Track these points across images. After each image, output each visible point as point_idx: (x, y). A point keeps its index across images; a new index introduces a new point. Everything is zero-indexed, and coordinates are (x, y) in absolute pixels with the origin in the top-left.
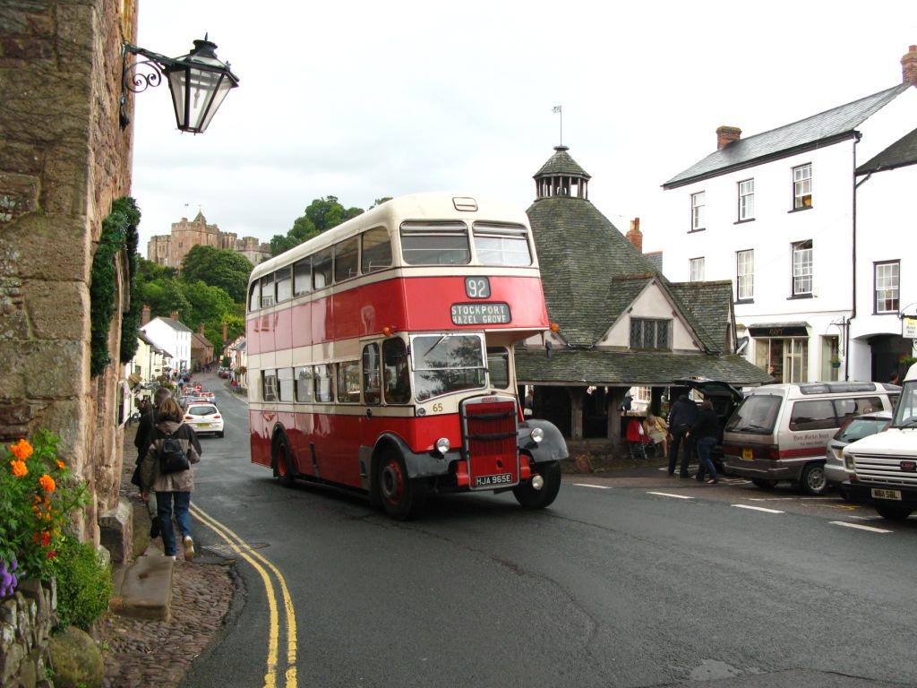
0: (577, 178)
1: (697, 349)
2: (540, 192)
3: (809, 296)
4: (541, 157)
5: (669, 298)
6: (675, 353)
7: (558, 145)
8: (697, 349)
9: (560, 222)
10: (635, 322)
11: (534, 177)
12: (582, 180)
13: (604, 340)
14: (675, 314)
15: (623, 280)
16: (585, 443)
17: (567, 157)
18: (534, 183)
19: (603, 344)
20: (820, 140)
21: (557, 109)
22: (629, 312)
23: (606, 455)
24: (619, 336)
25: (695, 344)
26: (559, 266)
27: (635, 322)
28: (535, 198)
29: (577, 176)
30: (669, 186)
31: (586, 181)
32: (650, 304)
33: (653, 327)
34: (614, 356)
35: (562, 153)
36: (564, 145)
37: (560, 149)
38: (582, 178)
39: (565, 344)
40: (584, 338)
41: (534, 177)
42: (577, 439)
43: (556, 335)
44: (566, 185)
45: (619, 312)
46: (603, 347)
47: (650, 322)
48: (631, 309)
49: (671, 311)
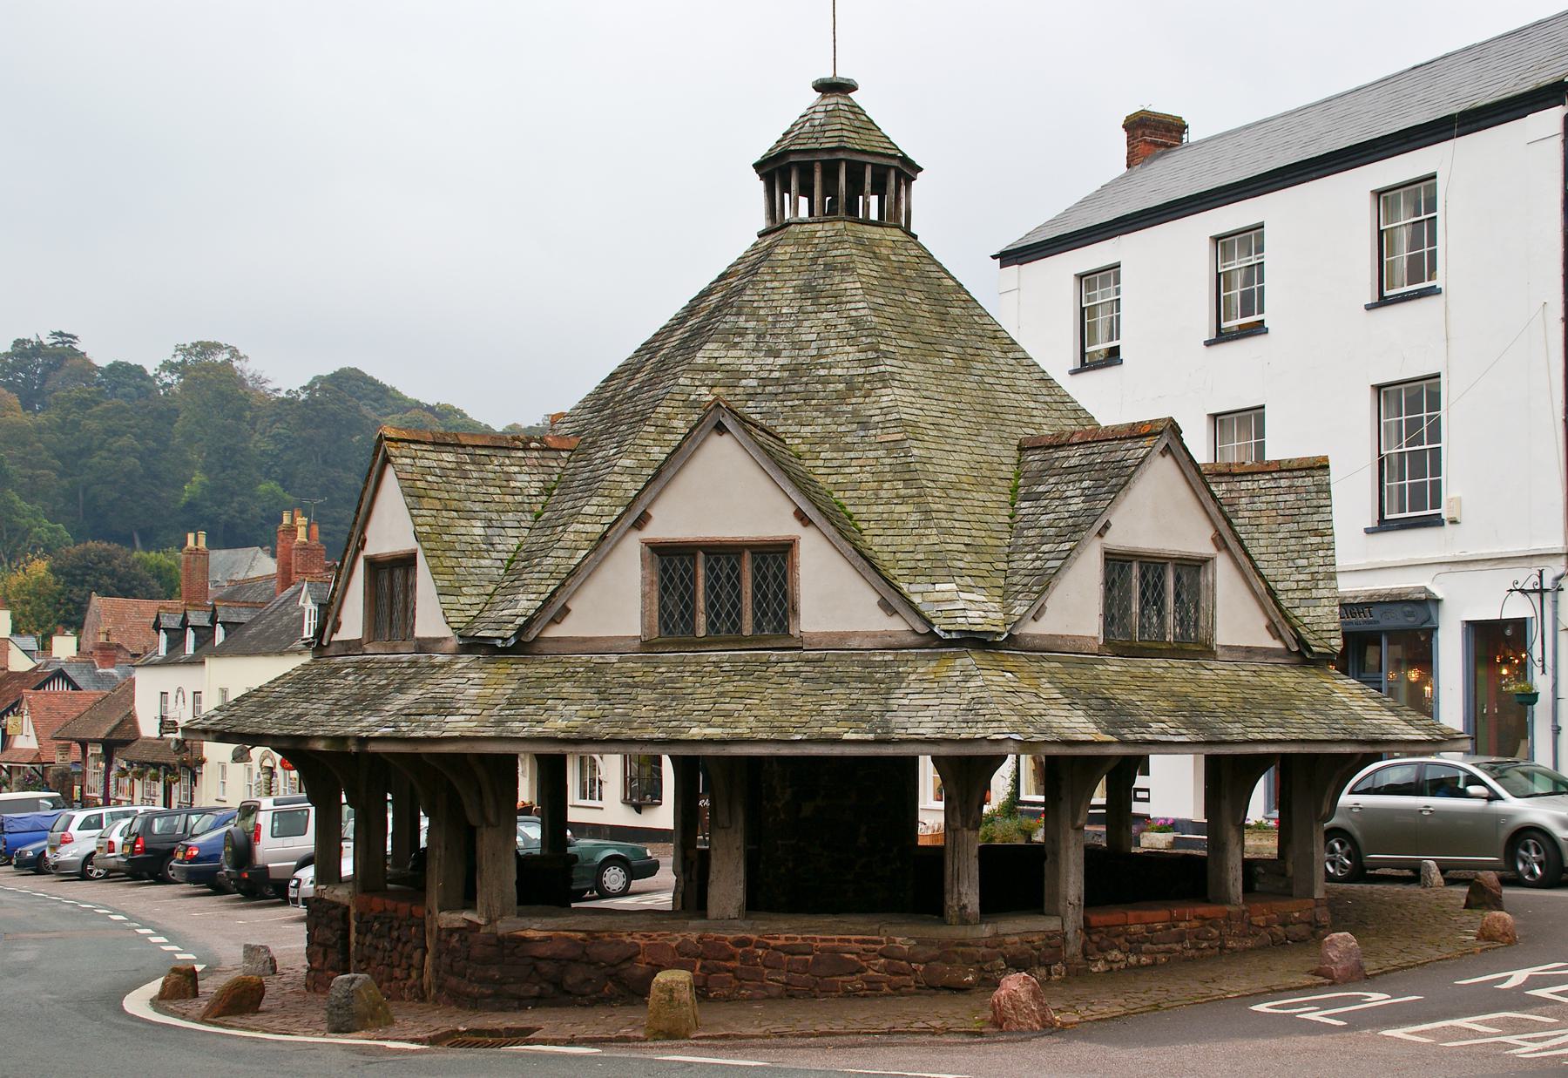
0: (889, 168)
1: (1278, 645)
3: (1435, 522)
4: (780, 110)
5: (1205, 496)
7: (827, 74)
8: (1278, 645)
9: (851, 284)
10: (1116, 563)
12: (899, 174)
14: (1219, 542)
16: (986, 930)
17: (856, 110)
19: (1031, 629)
20: (1463, 114)
22: (1100, 535)
23: (1048, 966)
25: (1273, 629)
27: (1116, 563)
28: (762, 223)
29: (885, 161)
30: (1008, 257)
31: (910, 180)
32: (1156, 517)
33: (1161, 576)
36: (844, 74)
37: (833, 88)
38: (898, 172)
40: (975, 609)
43: (895, 601)
44: (856, 188)
45: (1074, 531)
46: (1034, 637)
47: (1153, 565)
48: (1107, 526)
49: (1210, 532)
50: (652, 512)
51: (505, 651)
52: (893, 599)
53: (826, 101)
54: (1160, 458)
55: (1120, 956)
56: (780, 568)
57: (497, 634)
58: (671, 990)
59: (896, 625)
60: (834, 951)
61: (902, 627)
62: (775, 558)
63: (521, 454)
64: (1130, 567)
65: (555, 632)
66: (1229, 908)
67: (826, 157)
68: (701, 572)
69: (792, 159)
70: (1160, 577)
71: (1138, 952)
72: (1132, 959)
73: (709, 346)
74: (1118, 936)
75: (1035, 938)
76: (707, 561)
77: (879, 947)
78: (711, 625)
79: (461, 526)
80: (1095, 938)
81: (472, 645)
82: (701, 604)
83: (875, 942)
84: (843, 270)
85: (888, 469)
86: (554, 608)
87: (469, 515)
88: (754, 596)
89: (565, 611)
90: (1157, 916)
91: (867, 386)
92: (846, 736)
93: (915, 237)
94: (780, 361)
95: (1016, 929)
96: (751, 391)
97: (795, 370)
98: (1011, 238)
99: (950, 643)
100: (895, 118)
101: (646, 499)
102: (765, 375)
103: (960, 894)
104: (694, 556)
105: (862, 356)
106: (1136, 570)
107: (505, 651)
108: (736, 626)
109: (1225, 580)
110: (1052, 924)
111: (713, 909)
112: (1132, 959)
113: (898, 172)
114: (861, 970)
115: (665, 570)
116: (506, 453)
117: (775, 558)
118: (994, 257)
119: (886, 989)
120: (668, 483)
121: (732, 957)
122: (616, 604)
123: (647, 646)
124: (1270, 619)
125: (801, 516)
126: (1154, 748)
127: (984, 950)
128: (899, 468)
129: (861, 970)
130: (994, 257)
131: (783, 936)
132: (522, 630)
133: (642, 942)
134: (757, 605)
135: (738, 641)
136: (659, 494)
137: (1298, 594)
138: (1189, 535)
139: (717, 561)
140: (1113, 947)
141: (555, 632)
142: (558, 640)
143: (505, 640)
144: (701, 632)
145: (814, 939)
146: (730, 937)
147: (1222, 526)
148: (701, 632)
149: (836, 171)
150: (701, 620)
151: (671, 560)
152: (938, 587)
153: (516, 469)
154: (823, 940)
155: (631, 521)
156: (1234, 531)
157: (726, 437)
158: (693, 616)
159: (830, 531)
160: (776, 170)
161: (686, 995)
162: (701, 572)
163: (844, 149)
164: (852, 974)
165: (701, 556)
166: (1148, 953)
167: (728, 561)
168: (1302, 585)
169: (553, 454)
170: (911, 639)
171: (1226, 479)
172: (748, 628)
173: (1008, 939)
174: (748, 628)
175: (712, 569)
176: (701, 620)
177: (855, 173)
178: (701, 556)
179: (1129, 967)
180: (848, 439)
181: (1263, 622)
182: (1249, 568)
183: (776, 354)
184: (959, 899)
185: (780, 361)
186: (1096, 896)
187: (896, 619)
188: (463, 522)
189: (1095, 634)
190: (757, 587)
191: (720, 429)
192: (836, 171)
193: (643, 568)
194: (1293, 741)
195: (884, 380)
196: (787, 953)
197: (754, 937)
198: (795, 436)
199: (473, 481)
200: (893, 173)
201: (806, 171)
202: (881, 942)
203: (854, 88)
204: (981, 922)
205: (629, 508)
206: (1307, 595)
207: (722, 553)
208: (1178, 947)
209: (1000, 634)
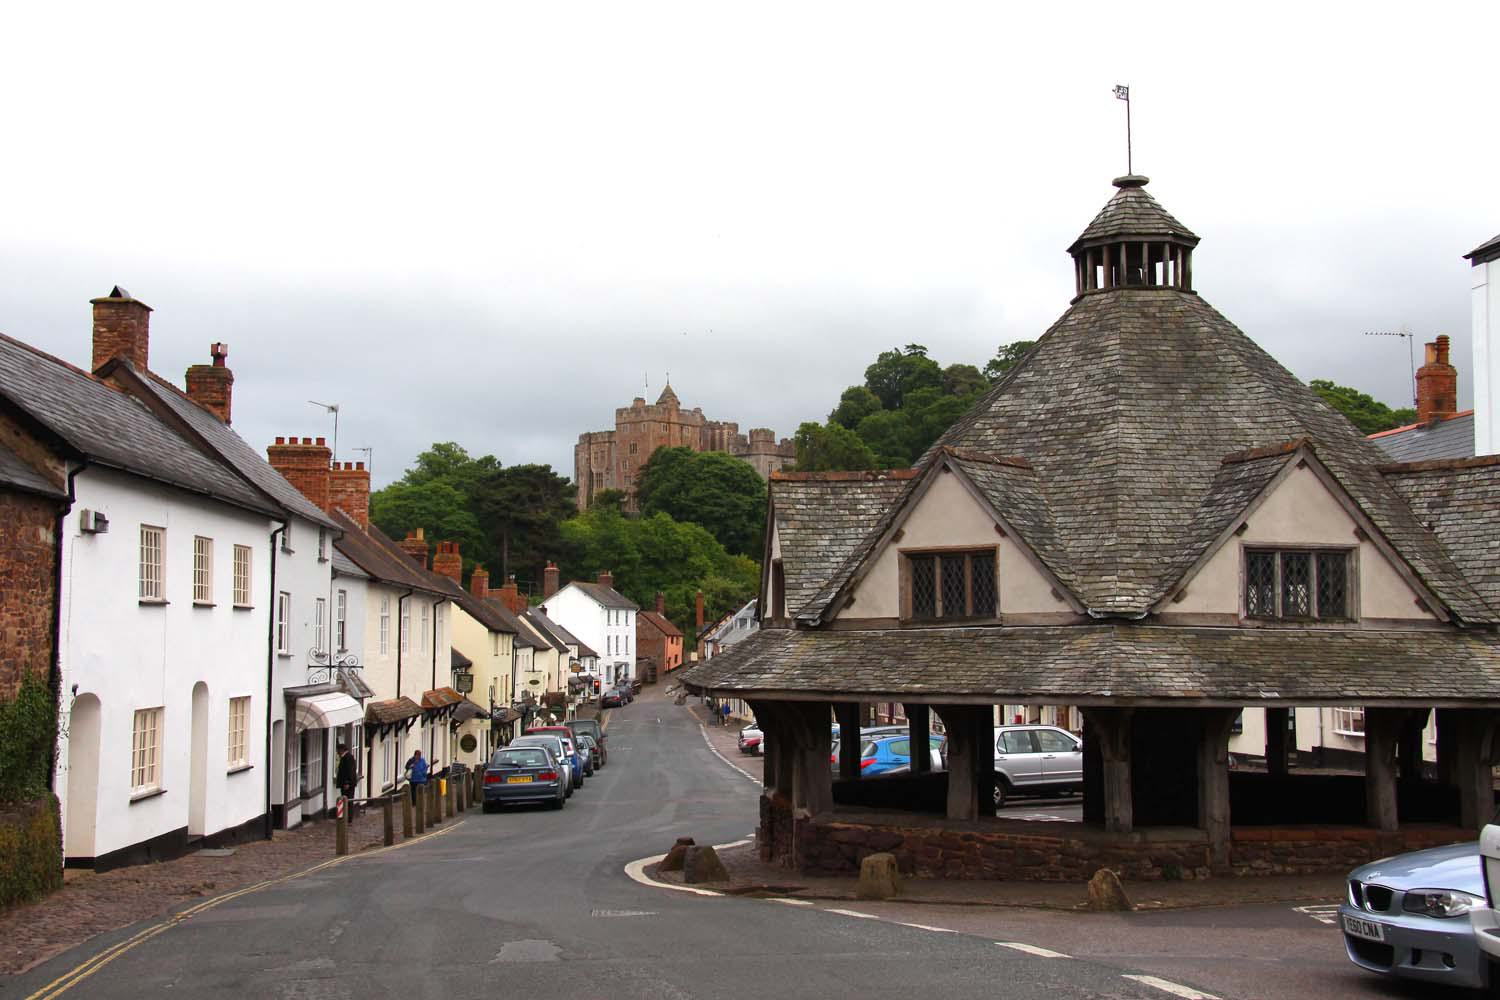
1: (1428, 616)
2: (1085, 279)
4: (1087, 203)
6: (1365, 626)
7: (1123, 173)
8: (1428, 616)
9: (1112, 342)
11: (1069, 250)
13: (1177, 600)
14: (1361, 534)
15: (1242, 462)
16: (1137, 838)
17: (1144, 199)
18: (1071, 262)
19: (1173, 608)
21: (1122, 92)
24: (1217, 589)
25: (1421, 603)
26: (1097, 440)
31: (1187, 252)
34: (1207, 637)
35: (1131, 193)
37: (1130, 184)
38: (1183, 244)
39: (1081, 611)
41: (1069, 250)
42: (1118, 830)
43: (1062, 591)
45: (1215, 535)
48: (1244, 527)
49: (1353, 527)
50: (906, 529)
51: (815, 628)
52: (1062, 590)
53: (1124, 195)
54: (1297, 470)
55: (1264, 865)
56: (990, 567)
57: (811, 617)
58: (873, 867)
59: (1064, 608)
60: (1027, 848)
61: (1067, 609)
62: (985, 558)
63: (871, 485)
64: (1273, 559)
65: (845, 615)
66: (1379, 832)
67: (1110, 241)
68: (938, 571)
69: (1086, 245)
70: (1303, 564)
71: (1284, 864)
72: (1278, 868)
73: (1005, 397)
74: (1264, 849)
75: (1180, 845)
76: (942, 563)
77: (1058, 846)
78: (945, 608)
79: (814, 540)
80: (1240, 849)
81: (803, 626)
82: (938, 595)
83: (1056, 842)
84: (1112, 330)
85: (1096, 487)
86: (847, 596)
87: (819, 533)
88: (973, 588)
89: (851, 601)
90: (1305, 836)
91: (1102, 422)
92: (998, 691)
93: (1195, 293)
94: (1048, 406)
95: (1165, 840)
96: (1022, 430)
97: (1056, 413)
98: (1475, 246)
99: (1101, 621)
100: (1177, 198)
101: (899, 519)
102: (1033, 417)
103: (1114, 809)
104: (933, 559)
105: (1104, 399)
106: (1278, 560)
107: (815, 628)
108: (962, 609)
109: (1370, 568)
110: (1195, 835)
111: (951, 813)
112: (1278, 868)
113: (1183, 244)
114: (1045, 863)
115: (916, 570)
116: (858, 485)
117: (985, 558)
118: (1466, 257)
119: (1062, 878)
120: (913, 509)
121: (960, 848)
122: (884, 594)
123: (903, 623)
124: (1418, 595)
125: (999, 529)
126: (1244, 703)
127: (1132, 853)
128: (1104, 487)
129: (1045, 863)
130: (1466, 257)
131: (997, 835)
132: (823, 615)
133: (906, 835)
134: (975, 594)
135: (963, 620)
136: (909, 515)
137: (1483, 572)
138: (1330, 528)
139: (949, 563)
140: (1258, 857)
141: (845, 615)
142: (848, 620)
143: (814, 620)
144: (939, 614)
145: (1016, 838)
146: (961, 834)
147: (1363, 522)
148: (939, 614)
149: (1131, 248)
150: (939, 605)
151: (918, 562)
152: (1104, 578)
153: (864, 496)
154: (1022, 839)
155: (890, 536)
156: (1374, 525)
157: (950, 475)
158: (934, 603)
159: (1017, 539)
160: (1085, 252)
161: (884, 869)
162: (938, 571)
163: (1121, 234)
164: (1039, 865)
165: (938, 561)
166: (1292, 864)
167: (926, 564)
168: (1489, 564)
169: (896, 483)
170: (1074, 619)
171: (1447, 473)
172: (969, 612)
173: (1154, 845)
174: (969, 612)
175: (946, 569)
176: (939, 605)
177: (1134, 249)
178: (938, 561)
179: (1274, 874)
180: (1077, 466)
181: (1412, 598)
182: (1392, 553)
183: (1045, 400)
184: (1113, 814)
185: (1048, 406)
186: (1241, 815)
187: (1063, 604)
188: (816, 537)
189: (1234, 610)
190: (975, 580)
191: (946, 469)
192: (1131, 248)
193: (900, 569)
194: (1388, 698)
195: (1115, 415)
196: (997, 847)
197: (976, 834)
198: (1043, 464)
199: (830, 507)
200: (1167, 247)
201: (1114, 251)
202: (1060, 843)
203: (1145, 182)
204: (1134, 831)
205: (888, 526)
206: (1490, 572)
207: (951, 557)
208: (1325, 861)
209: (1142, 614)
